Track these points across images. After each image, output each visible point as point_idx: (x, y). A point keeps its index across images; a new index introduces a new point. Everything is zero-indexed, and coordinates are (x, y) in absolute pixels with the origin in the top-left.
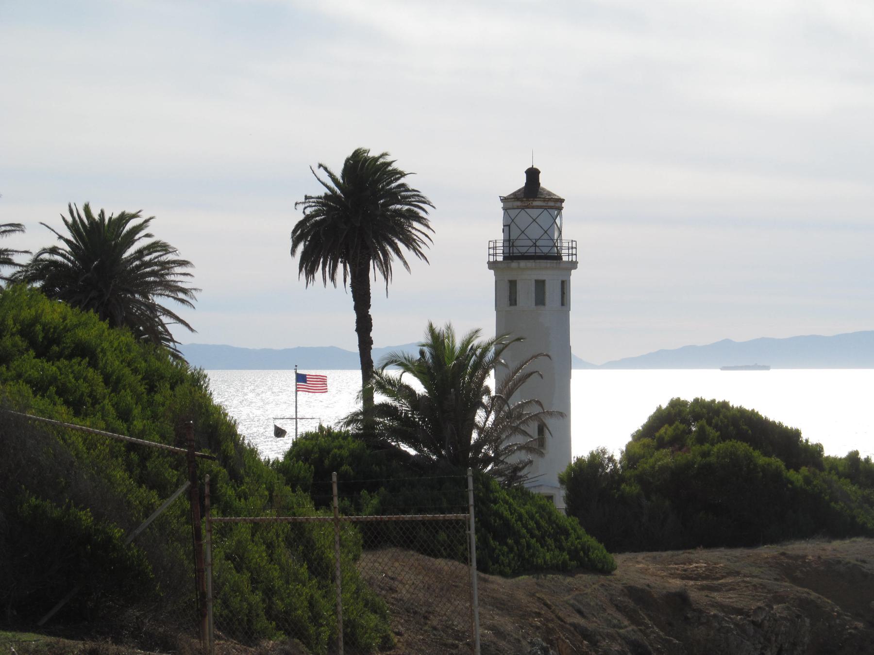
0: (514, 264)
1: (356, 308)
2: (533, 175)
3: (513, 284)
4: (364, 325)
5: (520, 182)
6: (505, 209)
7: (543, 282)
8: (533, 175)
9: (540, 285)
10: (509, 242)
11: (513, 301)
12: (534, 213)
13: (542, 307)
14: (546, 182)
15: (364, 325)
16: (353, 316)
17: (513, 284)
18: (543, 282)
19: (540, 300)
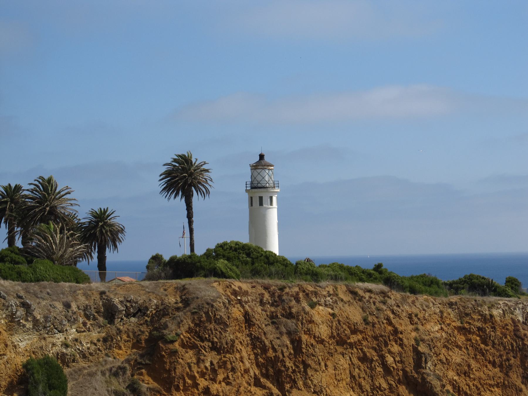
0: (253, 190)
1: (187, 209)
2: (262, 157)
3: (251, 198)
4: (190, 216)
5: (258, 159)
6: (251, 169)
7: (262, 197)
8: (262, 157)
9: (261, 198)
10: (252, 183)
11: (252, 205)
12: (259, 171)
13: (261, 207)
14: (267, 159)
15: (190, 216)
16: (186, 212)
17: (251, 198)
18: (262, 197)
19: (261, 204)
